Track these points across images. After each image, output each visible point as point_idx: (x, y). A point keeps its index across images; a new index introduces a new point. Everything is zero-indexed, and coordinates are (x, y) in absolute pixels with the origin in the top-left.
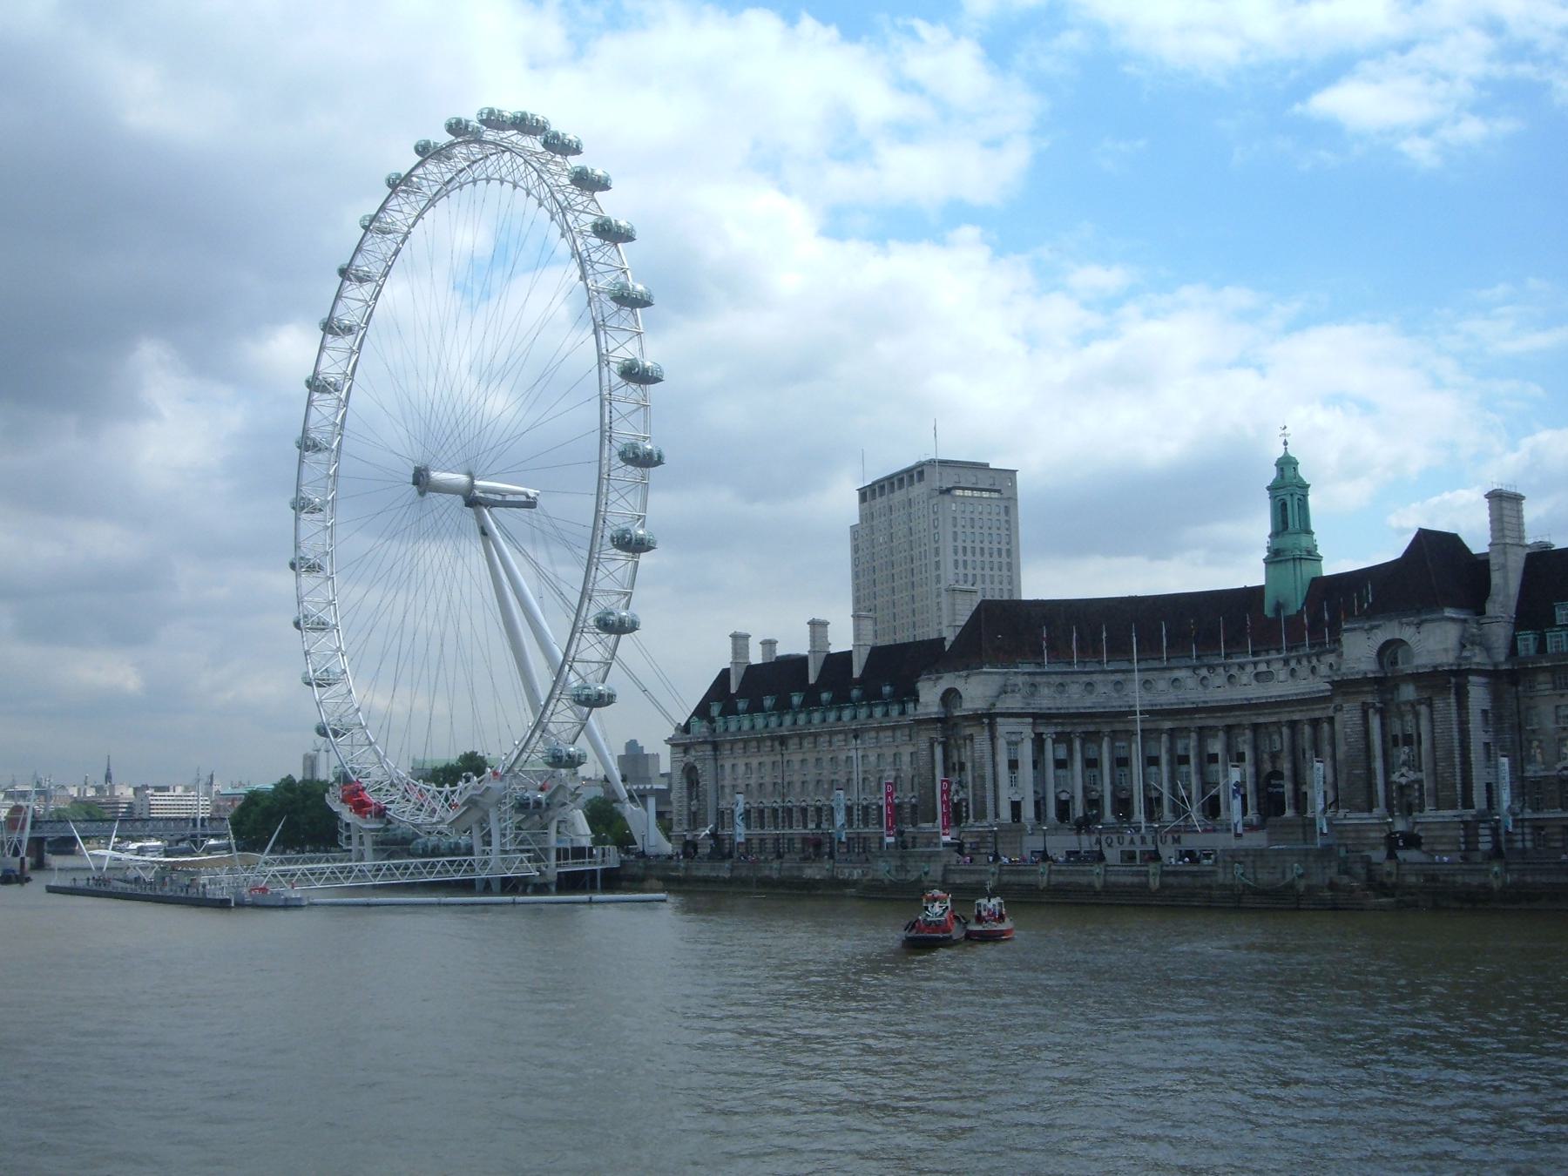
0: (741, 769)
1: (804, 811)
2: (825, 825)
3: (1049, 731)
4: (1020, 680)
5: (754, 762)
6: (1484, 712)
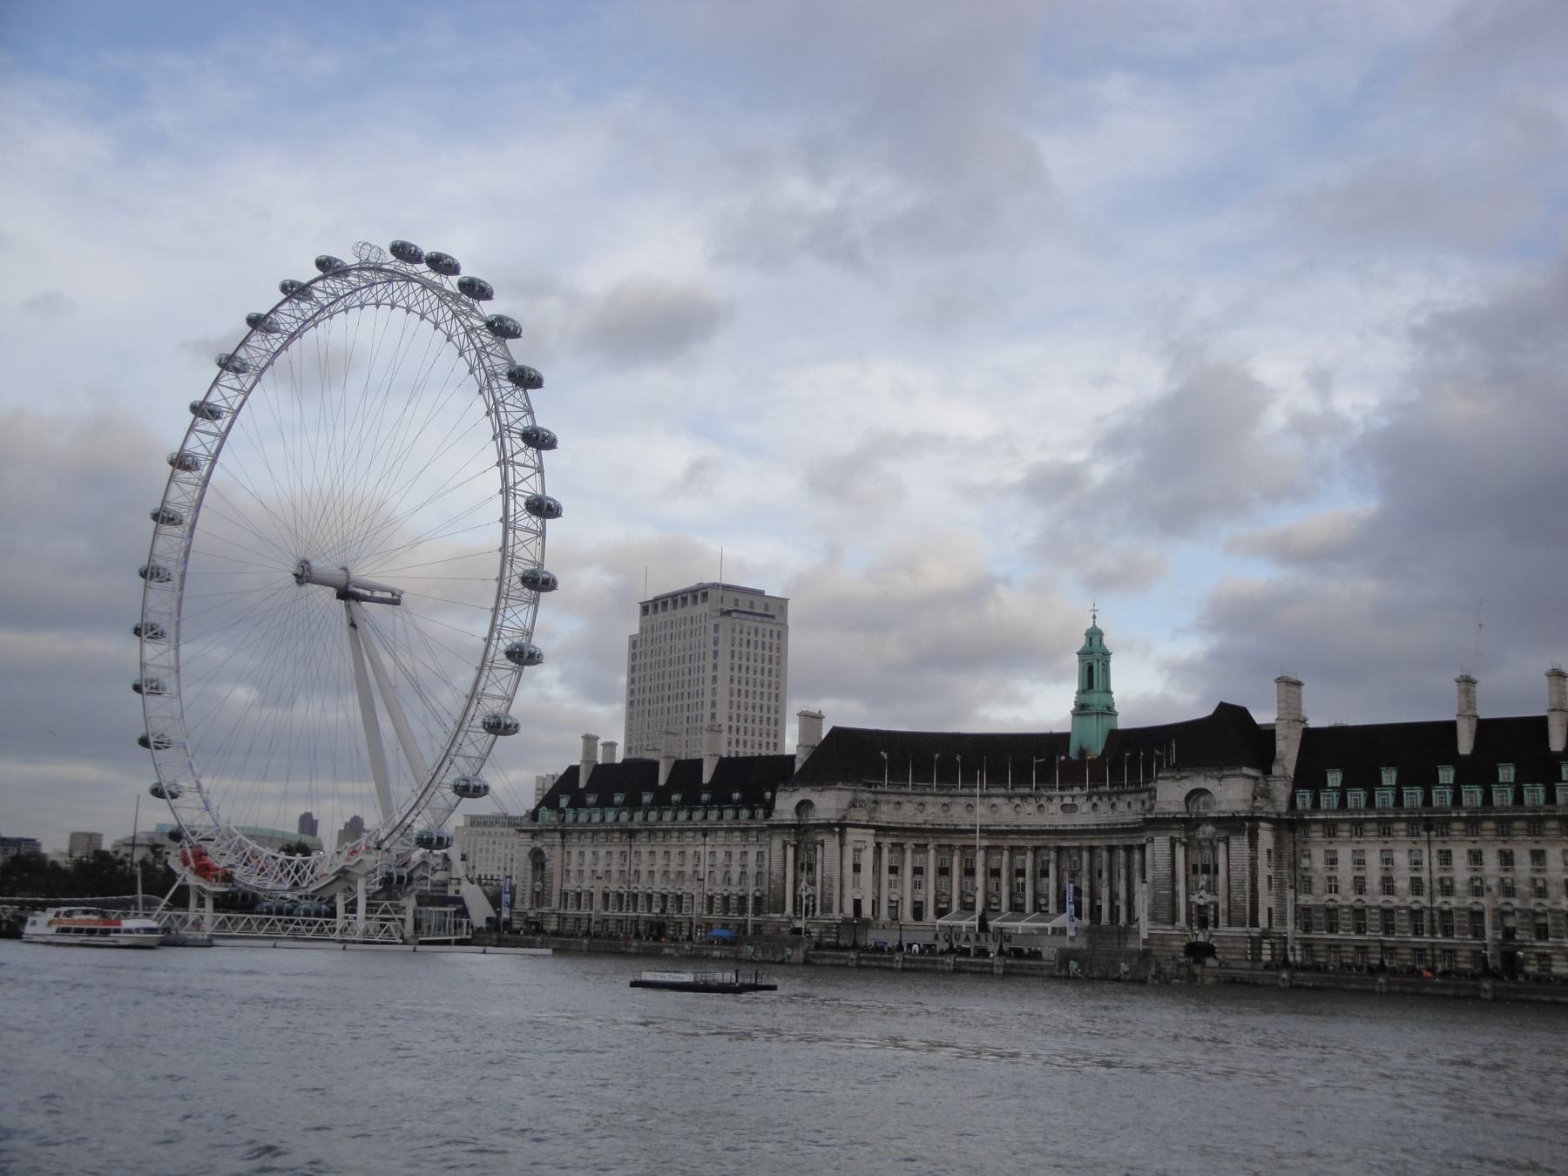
0: (589, 856)
1: (649, 897)
2: (671, 911)
3: (887, 842)
4: (866, 796)
6: (1269, 851)
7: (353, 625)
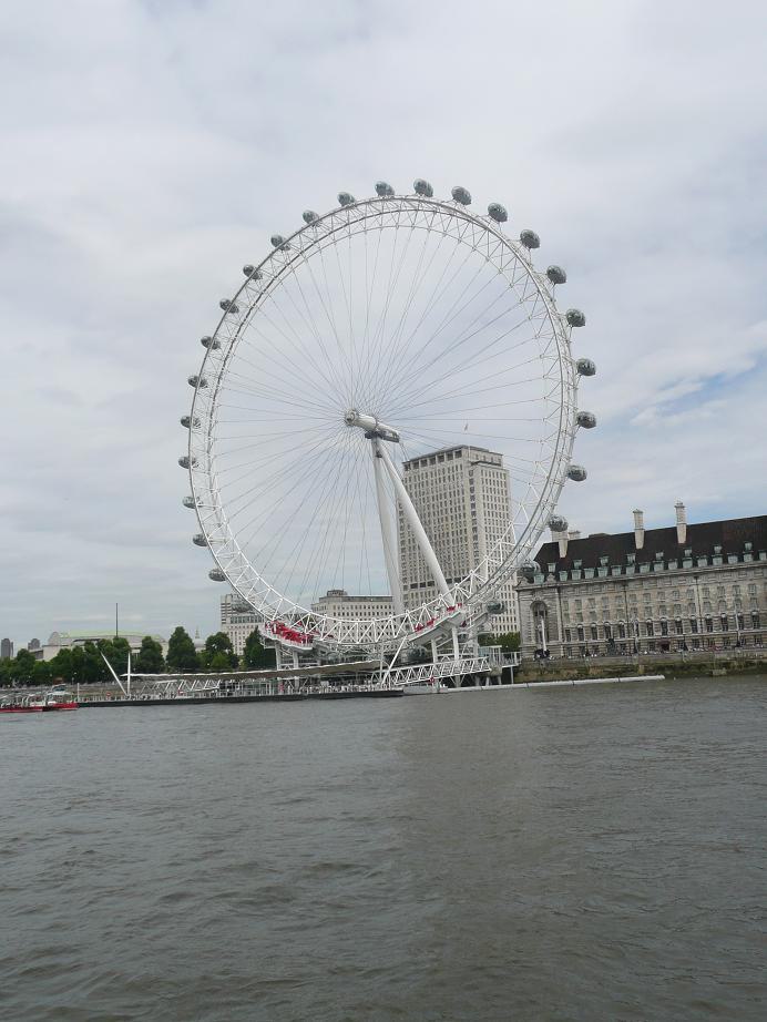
0: (585, 602)
2: (671, 633)
5: (598, 598)
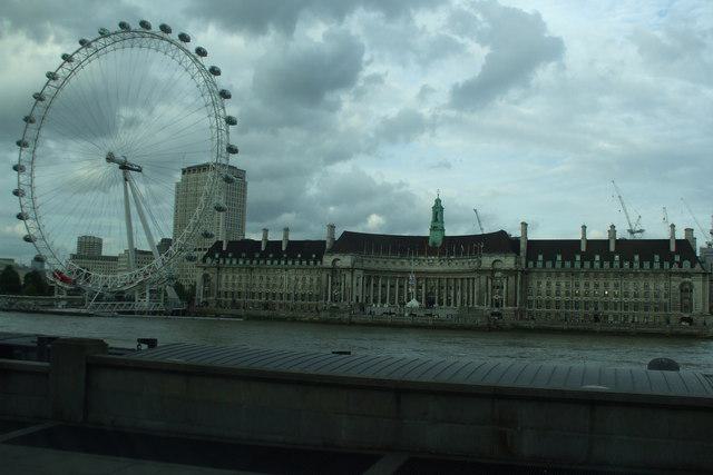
0: (230, 278)
7: (126, 180)
